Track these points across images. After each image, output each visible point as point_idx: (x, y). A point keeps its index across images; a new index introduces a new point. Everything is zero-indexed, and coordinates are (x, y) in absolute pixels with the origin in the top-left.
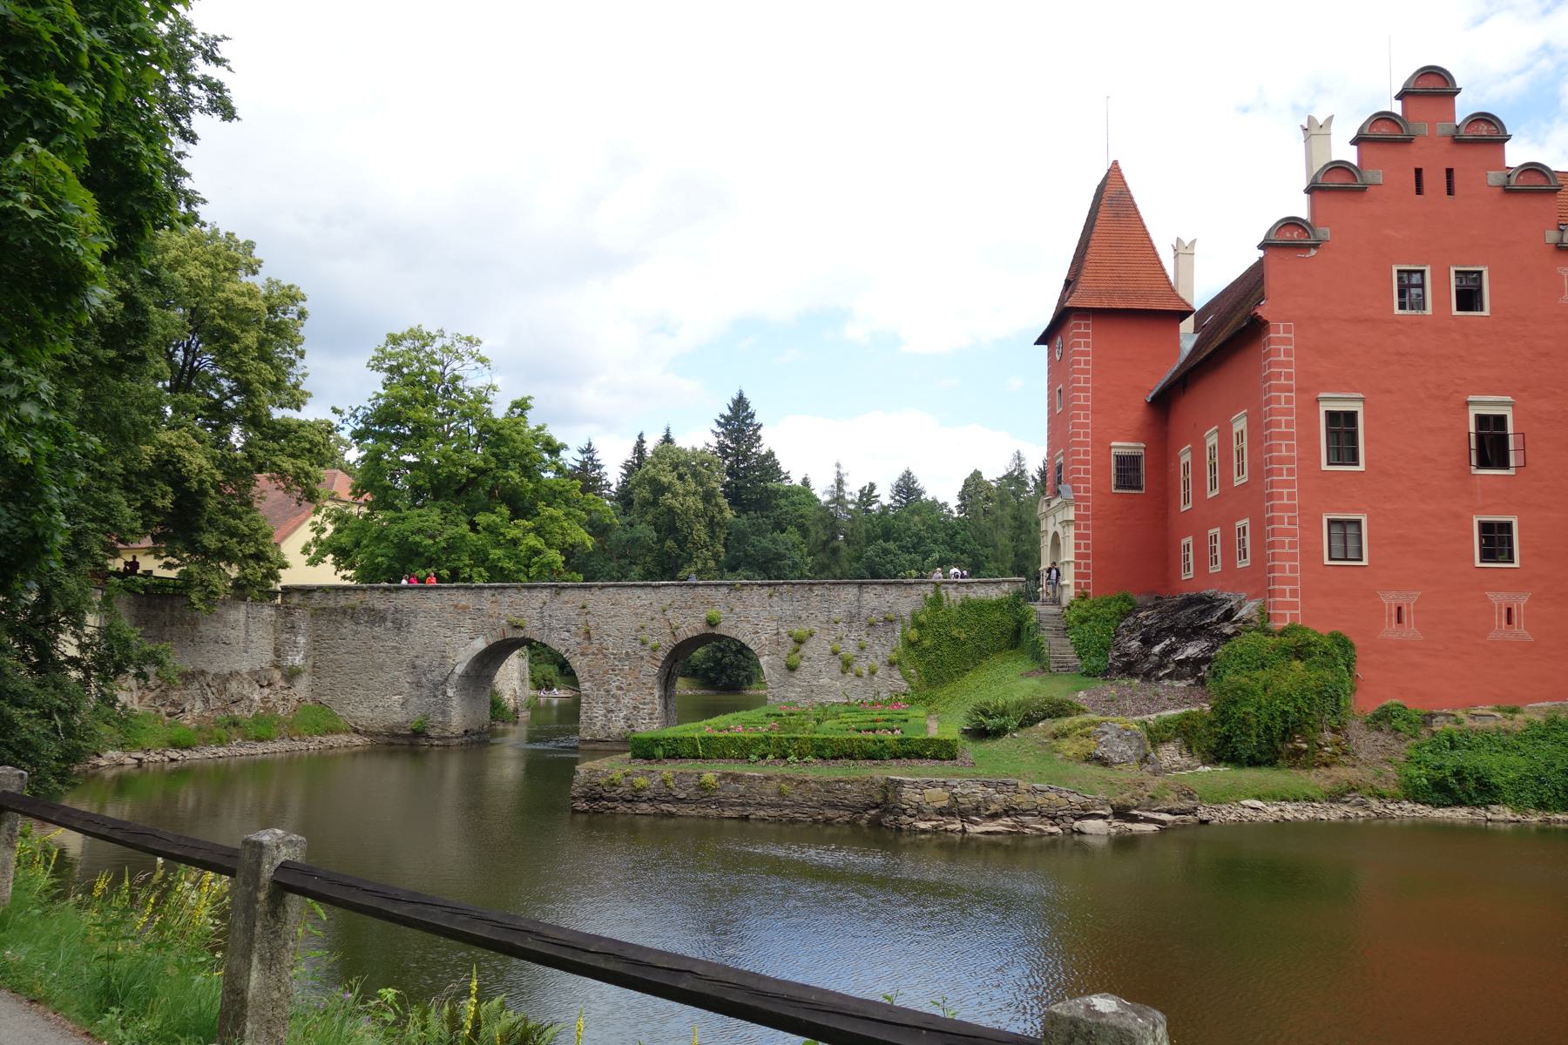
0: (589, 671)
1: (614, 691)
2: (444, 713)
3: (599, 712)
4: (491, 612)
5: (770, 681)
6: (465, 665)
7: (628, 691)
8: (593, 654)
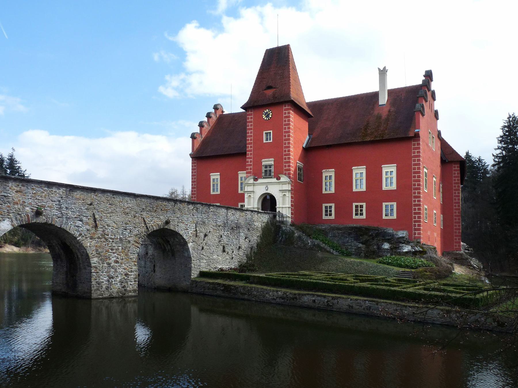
1: (113, 264)
3: (104, 279)
4: (16, 200)
8: (99, 238)
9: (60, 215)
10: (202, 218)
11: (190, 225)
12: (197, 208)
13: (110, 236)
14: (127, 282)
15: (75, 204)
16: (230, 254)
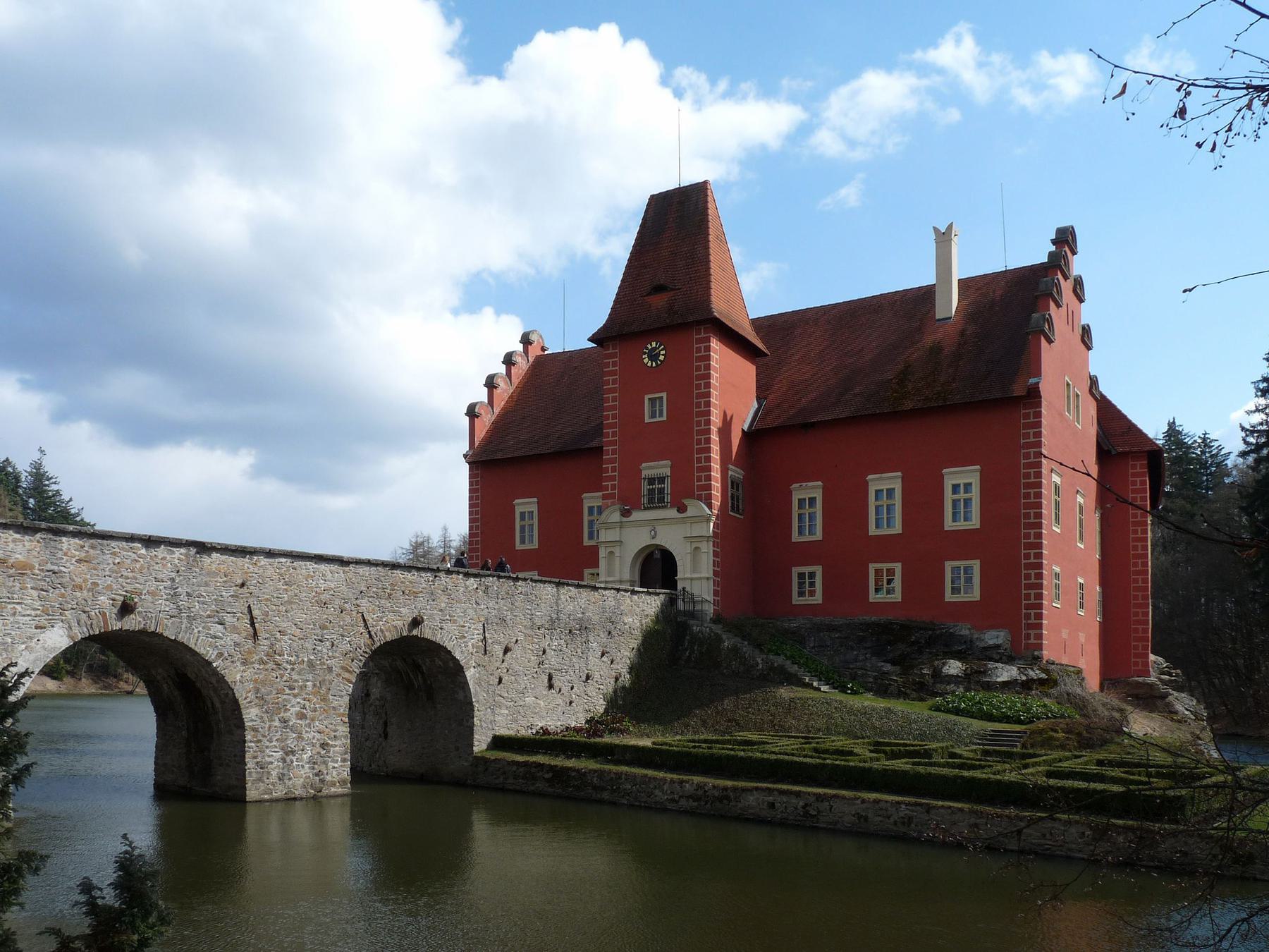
1: (293, 721)
3: (274, 756)
4: (78, 580)
8: (261, 662)
9: (174, 612)
10: (499, 610)
11: (469, 628)
13: (286, 657)
14: (325, 763)
15: (207, 585)
16: (566, 694)
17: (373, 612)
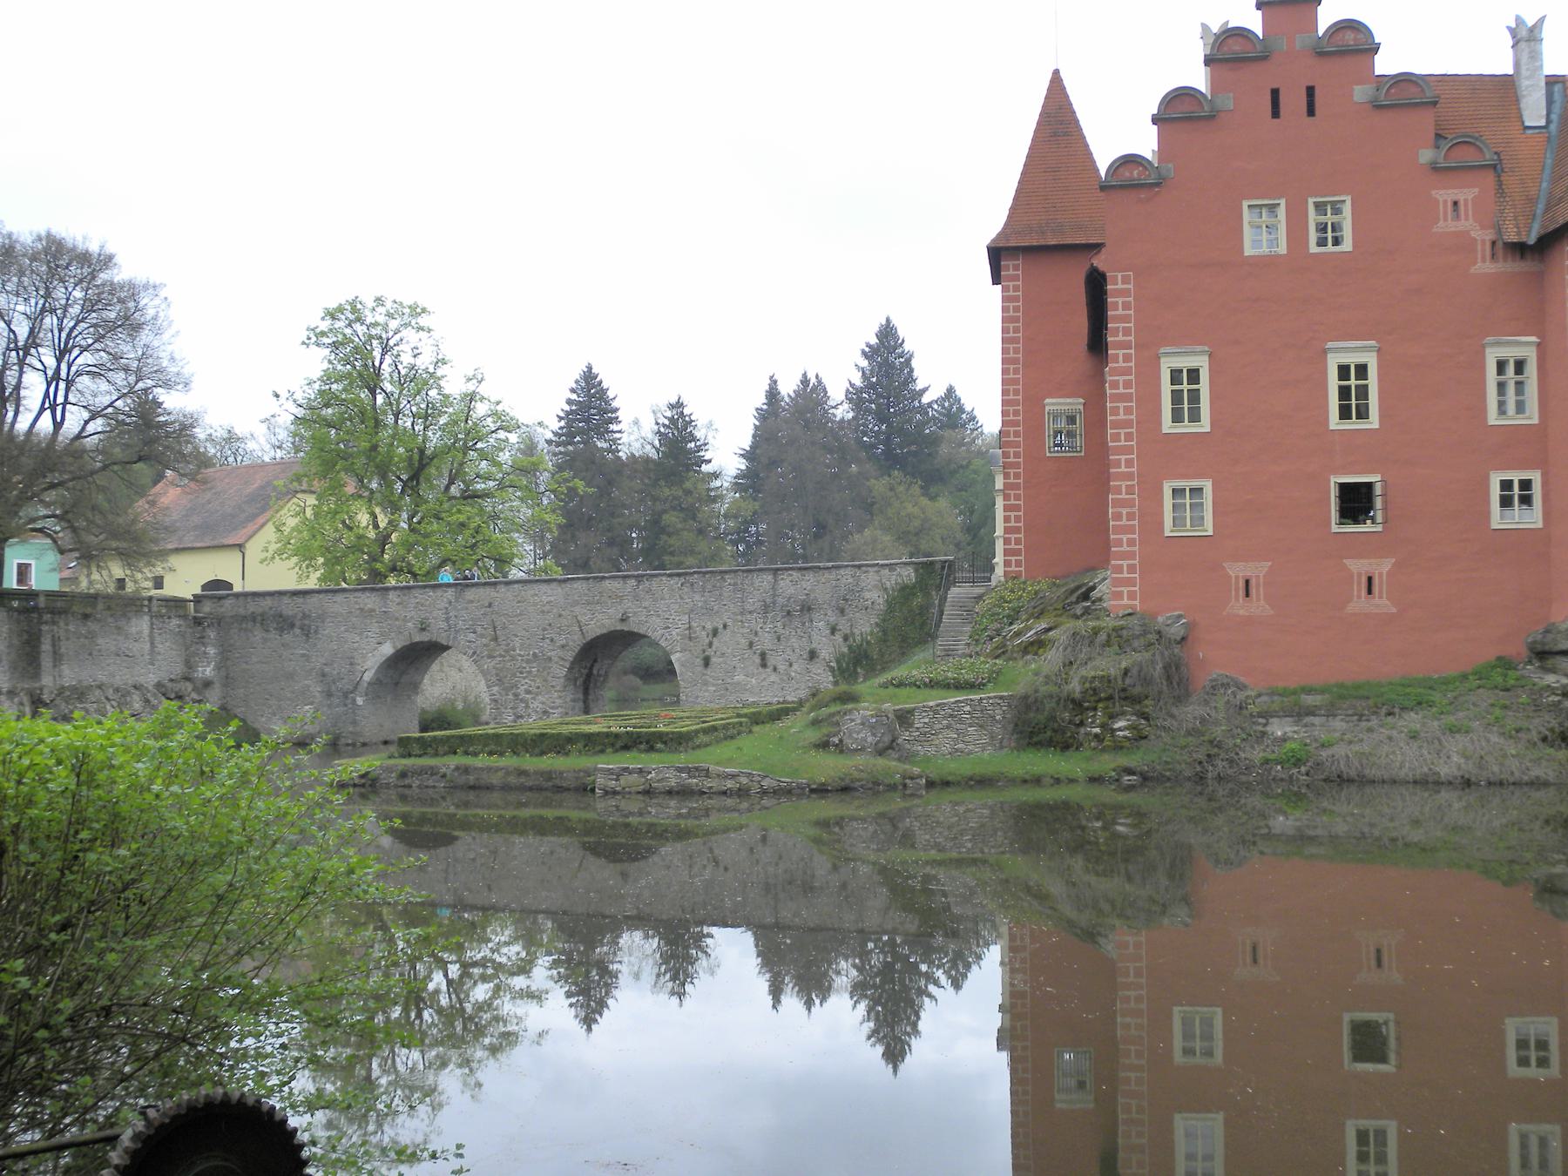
0: (497, 675)
2: (354, 723)
5: (683, 680)
6: (373, 671)
7: (537, 695)
8: (501, 656)
9: (446, 628)
12: (692, 585)
17: (585, 614)
